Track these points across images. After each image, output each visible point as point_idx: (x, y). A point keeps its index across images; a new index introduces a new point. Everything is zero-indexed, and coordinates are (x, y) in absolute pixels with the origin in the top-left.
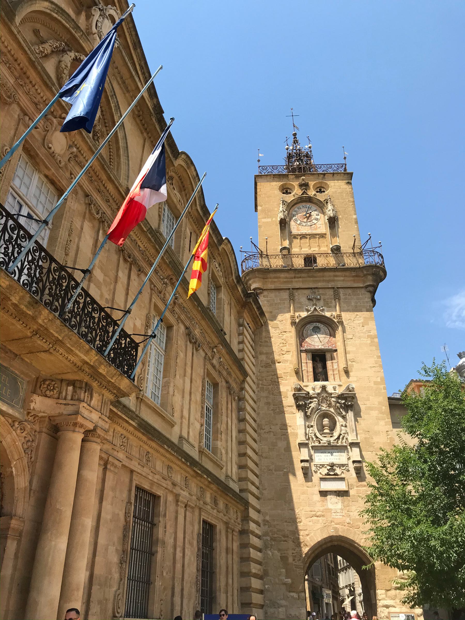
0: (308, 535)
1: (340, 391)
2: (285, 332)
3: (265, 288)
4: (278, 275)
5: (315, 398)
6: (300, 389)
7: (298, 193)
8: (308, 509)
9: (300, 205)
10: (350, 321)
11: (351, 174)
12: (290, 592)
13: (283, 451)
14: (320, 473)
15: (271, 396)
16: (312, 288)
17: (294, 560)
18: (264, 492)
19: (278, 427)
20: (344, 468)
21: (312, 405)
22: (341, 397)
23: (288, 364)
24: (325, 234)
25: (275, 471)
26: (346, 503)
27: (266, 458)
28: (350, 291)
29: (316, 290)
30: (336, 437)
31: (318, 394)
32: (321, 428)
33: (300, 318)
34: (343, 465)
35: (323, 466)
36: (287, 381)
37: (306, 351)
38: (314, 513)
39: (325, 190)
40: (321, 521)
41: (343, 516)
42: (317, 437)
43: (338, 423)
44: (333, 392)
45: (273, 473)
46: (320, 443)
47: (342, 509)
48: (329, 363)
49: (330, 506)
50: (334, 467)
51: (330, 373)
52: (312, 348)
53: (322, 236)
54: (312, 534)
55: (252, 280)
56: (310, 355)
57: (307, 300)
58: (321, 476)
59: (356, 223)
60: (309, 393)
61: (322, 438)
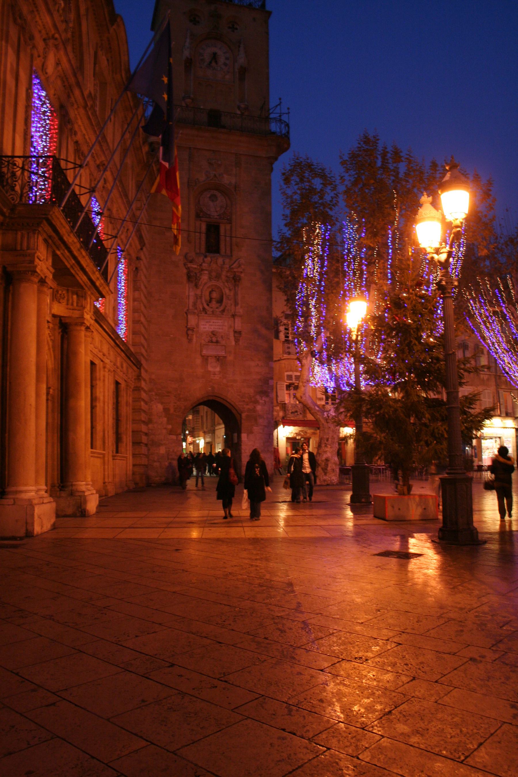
5: (206, 270)
11: (269, 13)
12: (170, 434)
17: (175, 411)
43: (224, 296)
47: (220, 372)
49: (210, 369)
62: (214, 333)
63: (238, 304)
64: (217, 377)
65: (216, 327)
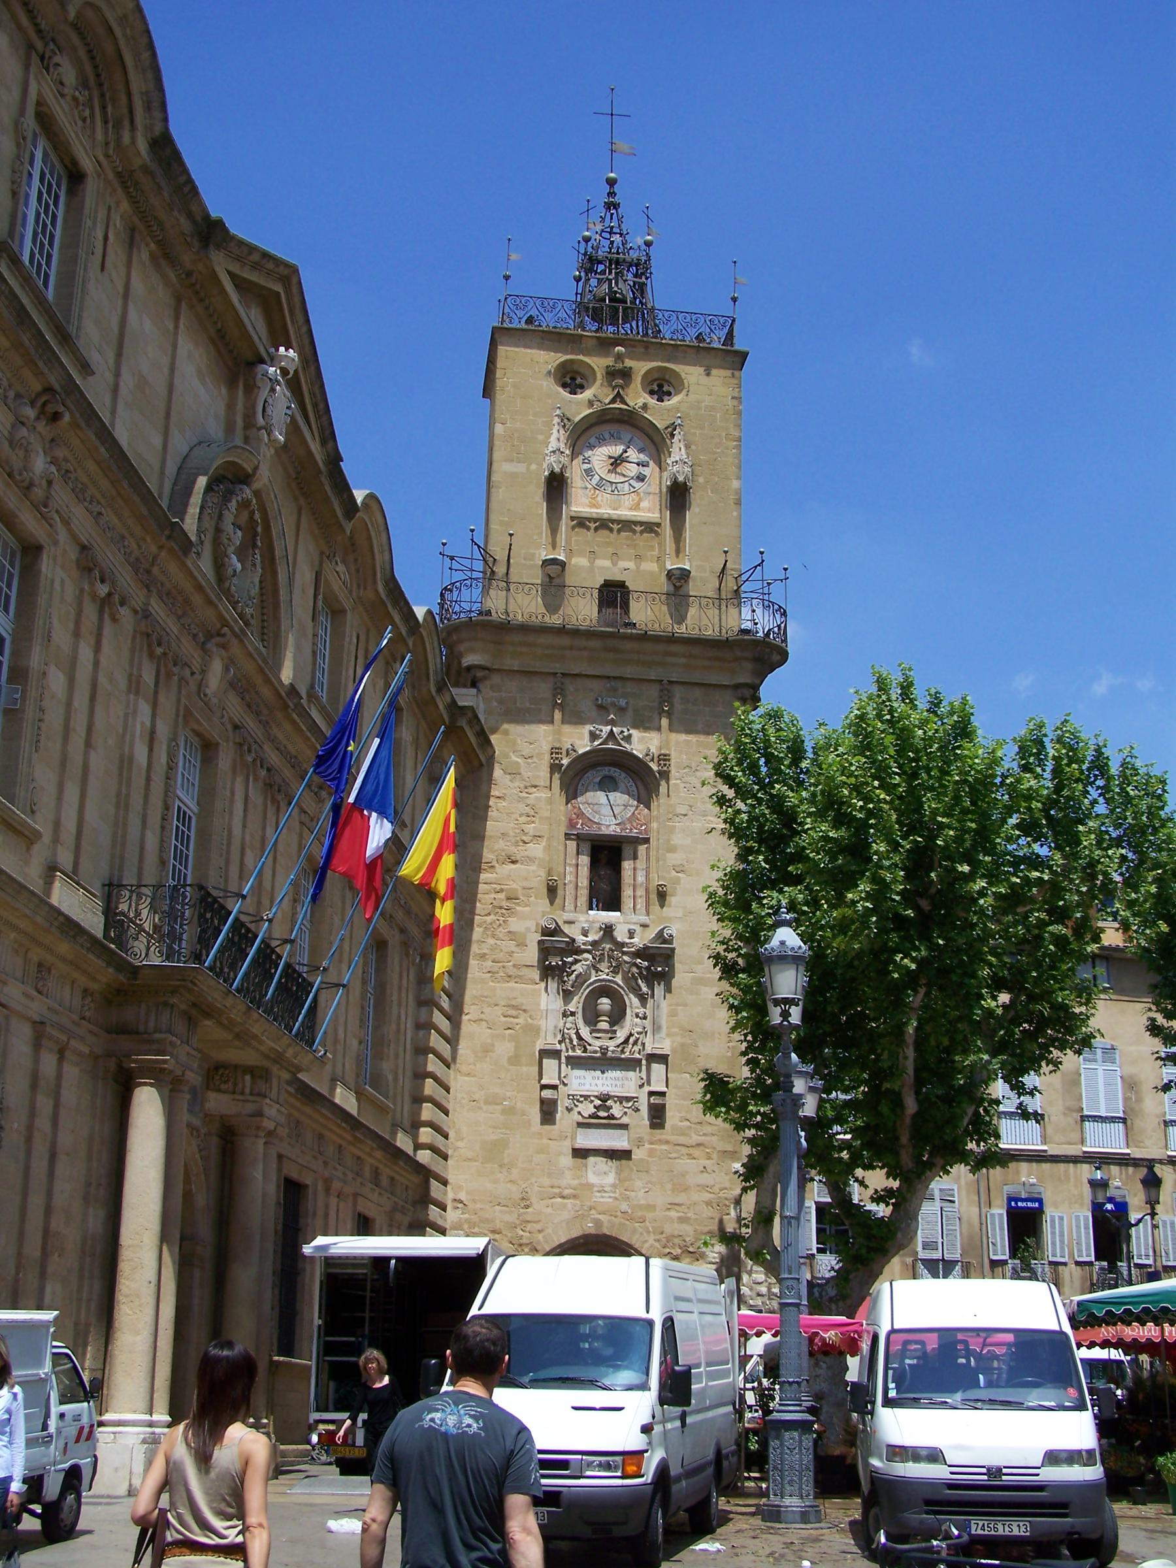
0: (540, 1231)
1: (638, 941)
2: (535, 787)
3: (496, 667)
4: (531, 638)
6: (557, 931)
7: (600, 397)
8: (546, 1181)
9: (606, 429)
10: (687, 770)
13: (506, 1064)
14: (579, 1113)
15: (491, 941)
16: (608, 677)
18: (460, 1144)
19: (499, 1011)
20: (630, 1104)
21: (579, 968)
22: (642, 953)
23: (534, 868)
24: (658, 525)
25: (486, 1102)
26: (625, 1174)
27: (469, 1075)
28: (697, 693)
29: (619, 684)
30: (621, 1040)
31: (595, 944)
32: (592, 1018)
33: (574, 755)
34: (628, 1099)
35: (586, 1097)
36: (527, 908)
37: (579, 838)
38: (557, 1190)
39: (672, 390)
40: (570, 1206)
41: (616, 1198)
42: (580, 1038)
43: (628, 1011)
44: (628, 941)
45: (480, 1108)
46: (585, 1051)
47: (614, 1186)
48: (627, 865)
49: (592, 1178)
50: (609, 1103)
51: (627, 893)
52: (594, 830)
53: (650, 528)
54: (550, 1230)
55: (467, 645)
56: (586, 847)
57: (594, 708)
58: (580, 1119)
59: (738, 503)
60: (573, 940)
61: (591, 1041)
62: (604, 1098)
63: (659, 1028)
64: (606, 1199)
65: (609, 1082)
